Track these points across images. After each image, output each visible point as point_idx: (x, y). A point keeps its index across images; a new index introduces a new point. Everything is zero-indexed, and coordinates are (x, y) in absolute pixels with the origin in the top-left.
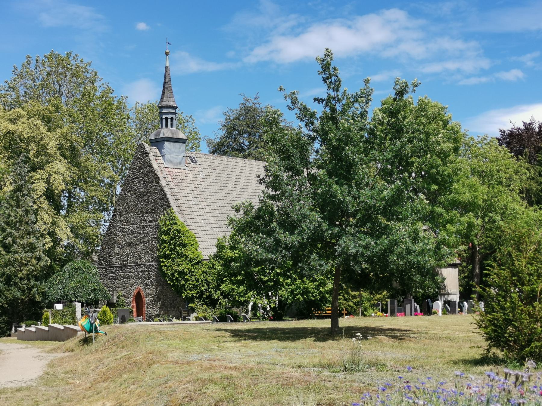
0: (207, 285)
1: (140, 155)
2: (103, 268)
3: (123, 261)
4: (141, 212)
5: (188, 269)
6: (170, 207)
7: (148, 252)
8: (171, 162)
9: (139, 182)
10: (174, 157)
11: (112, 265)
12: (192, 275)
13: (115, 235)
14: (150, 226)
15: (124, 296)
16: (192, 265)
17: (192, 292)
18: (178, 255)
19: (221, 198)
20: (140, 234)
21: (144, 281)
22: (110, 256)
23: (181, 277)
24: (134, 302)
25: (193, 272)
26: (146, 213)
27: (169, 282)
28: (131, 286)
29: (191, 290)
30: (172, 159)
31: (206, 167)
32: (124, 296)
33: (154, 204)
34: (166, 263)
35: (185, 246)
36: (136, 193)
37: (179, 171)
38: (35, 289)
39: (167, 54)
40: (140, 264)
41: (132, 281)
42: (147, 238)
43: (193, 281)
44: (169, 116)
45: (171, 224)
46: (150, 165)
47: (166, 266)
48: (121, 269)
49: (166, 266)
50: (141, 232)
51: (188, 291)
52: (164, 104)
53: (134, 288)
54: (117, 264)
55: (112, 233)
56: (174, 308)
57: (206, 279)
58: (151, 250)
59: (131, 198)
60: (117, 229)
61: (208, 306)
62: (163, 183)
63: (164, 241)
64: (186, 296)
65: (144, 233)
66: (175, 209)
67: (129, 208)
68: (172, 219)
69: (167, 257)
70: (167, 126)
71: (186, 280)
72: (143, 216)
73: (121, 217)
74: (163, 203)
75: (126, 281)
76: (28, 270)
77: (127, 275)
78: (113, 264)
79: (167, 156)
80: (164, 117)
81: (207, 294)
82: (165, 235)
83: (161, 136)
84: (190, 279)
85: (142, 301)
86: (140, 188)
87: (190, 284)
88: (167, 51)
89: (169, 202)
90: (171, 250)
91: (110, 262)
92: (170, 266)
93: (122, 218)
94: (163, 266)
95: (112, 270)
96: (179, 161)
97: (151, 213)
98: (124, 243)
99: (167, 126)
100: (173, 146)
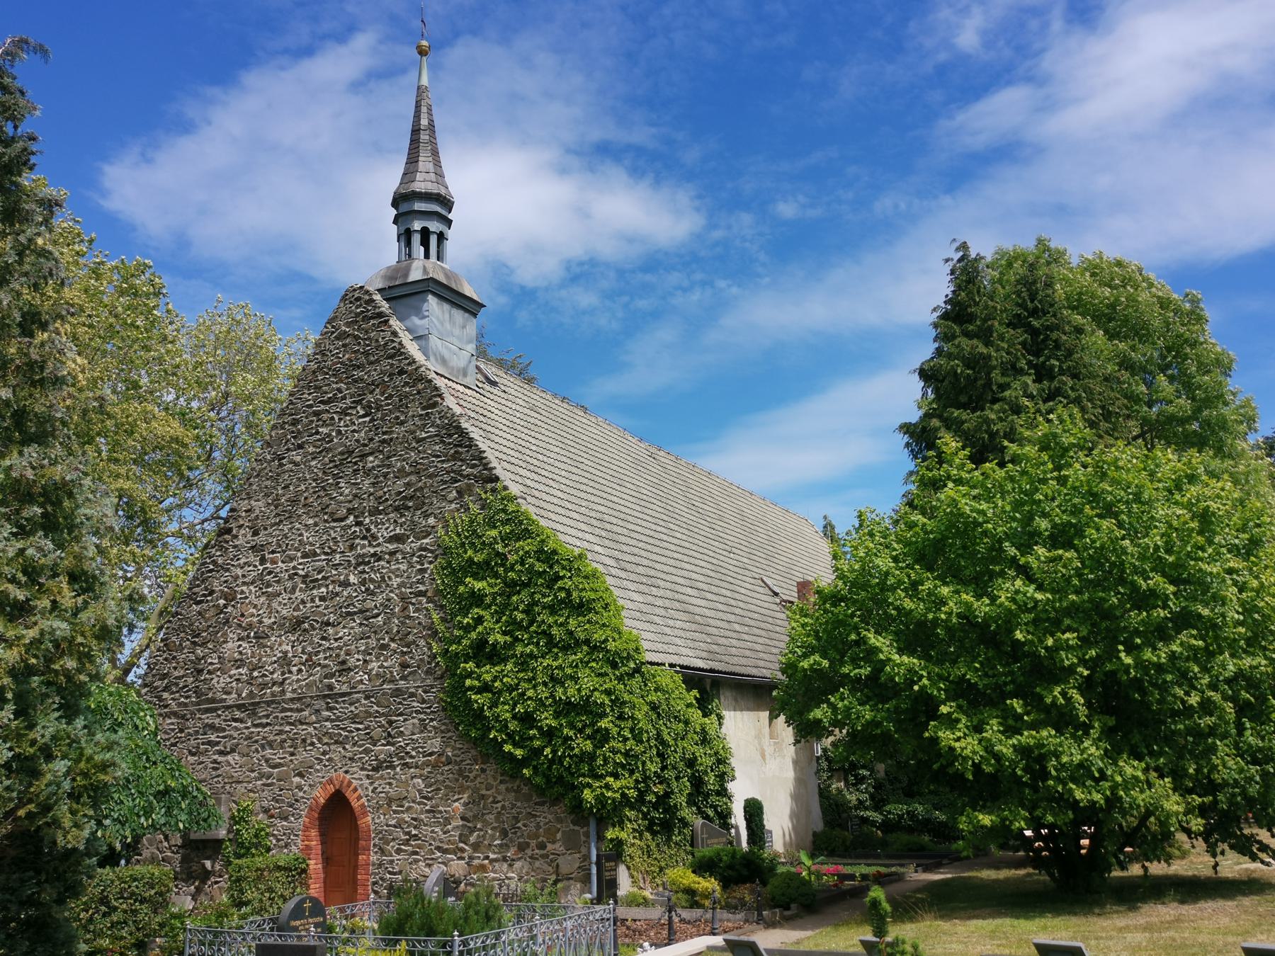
0: (660, 755)
1: (348, 324)
2: (167, 716)
3: (264, 686)
4: (350, 511)
5: (608, 692)
6: (497, 479)
7: (384, 647)
8: (444, 362)
9: (344, 413)
10: (450, 350)
11: (212, 705)
12: (621, 717)
13: (230, 597)
14: (392, 553)
15: (266, 811)
16: (620, 679)
17: (624, 782)
18: (551, 643)
19: (584, 487)
20: (346, 584)
21: (367, 751)
22: (200, 672)
23: (572, 726)
24: (314, 833)
25: (624, 703)
26: (374, 512)
27: (507, 748)
28: (301, 775)
29: (616, 776)
30: (446, 355)
31: (521, 402)
32: (266, 811)
33: (413, 478)
34: (488, 677)
35: (582, 608)
36: (328, 450)
37: (469, 392)
38: (61, 766)
39: (422, 52)
40: (345, 688)
41: (302, 755)
42: (380, 599)
43: (626, 739)
44: (434, 226)
45: (505, 539)
46: (400, 352)
47: (486, 688)
48: (254, 714)
49: (486, 688)
50: (352, 579)
51: (610, 780)
52: (420, 186)
53: (315, 778)
54: (231, 699)
55: (212, 593)
56: (522, 848)
57: (659, 735)
58: (403, 638)
59: (306, 466)
60: (236, 578)
61: (654, 834)
62: (450, 402)
63: (476, 599)
64: (601, 800)
65: (363, 583)
66: (515, 489)
67: (294, 502)
68: (507, 522)
69: (484, 652)
70: (427, 256)
71: (601, 738)
72: (358, 524)
73: (255, 533)
74: (459, 473)
75: (276, 756)
76: (36, 642)
77: (281, 732)
78: (213, 700)
79: (434, 341)
80: (417, 225)
81: (659, 789)
82: (476, 577)
83: (415, 275)
84: (615, 730)
85: (357, 826)
86: (355, 428)
87: (614, 751)
88: (424, 43)
89: (486, 466)
90: (513, 627)
91: (197, 692)
92: (511, 689)
93: (261, 539)
94: (471, 688)
95: (208, 719)
96: (462, 364)
97: (397, 509)
98: (267, 621)
99: (427, 256)
100: (447, 316)
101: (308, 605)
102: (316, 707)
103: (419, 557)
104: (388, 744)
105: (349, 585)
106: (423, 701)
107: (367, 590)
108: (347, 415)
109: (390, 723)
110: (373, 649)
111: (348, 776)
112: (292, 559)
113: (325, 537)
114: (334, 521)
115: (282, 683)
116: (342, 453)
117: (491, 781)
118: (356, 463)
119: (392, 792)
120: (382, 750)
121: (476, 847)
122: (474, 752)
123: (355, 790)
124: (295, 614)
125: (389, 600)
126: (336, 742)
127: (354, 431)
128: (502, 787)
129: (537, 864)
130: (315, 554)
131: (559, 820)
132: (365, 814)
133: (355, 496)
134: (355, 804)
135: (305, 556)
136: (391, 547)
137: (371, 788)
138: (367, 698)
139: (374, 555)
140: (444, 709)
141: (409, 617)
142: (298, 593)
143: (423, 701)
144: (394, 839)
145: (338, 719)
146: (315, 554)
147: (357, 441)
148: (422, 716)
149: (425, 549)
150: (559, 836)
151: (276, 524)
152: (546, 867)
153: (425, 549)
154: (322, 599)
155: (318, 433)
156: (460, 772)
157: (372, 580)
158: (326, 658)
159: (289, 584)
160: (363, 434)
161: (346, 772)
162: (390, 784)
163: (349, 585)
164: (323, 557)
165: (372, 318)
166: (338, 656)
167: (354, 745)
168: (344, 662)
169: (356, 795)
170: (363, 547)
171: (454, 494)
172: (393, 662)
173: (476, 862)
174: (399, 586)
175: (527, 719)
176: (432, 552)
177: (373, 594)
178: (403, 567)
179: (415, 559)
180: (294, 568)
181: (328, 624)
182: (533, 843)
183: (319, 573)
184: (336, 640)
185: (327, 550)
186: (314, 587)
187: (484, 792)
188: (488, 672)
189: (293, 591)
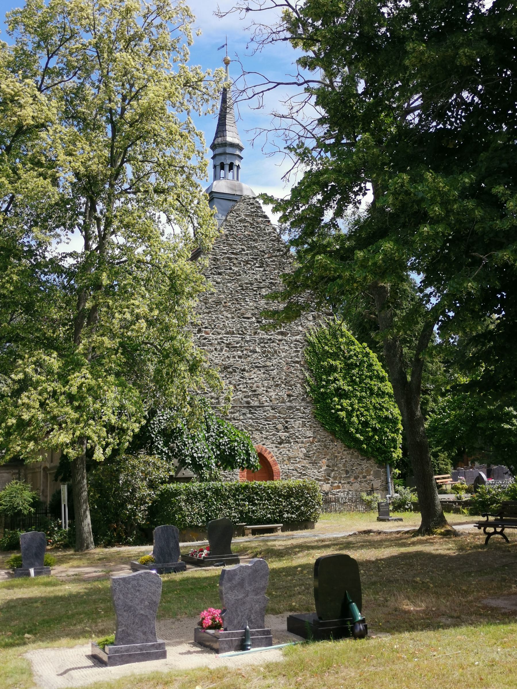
7: (277, 385)
20: (254, 352)
21: (274, 435)
40: (257, 404)
50: (258, 350)
56: (356, 478)
65: (264, 352)
67: (218, 303)
72: (258, 322)
101: (231, 359)
102: (244, 412)
103: (295, 344)
104: (285, 432)
105: (256, 352)
106: (304, 413)
107: (267, 356)
108: (248, 263)
109: (287, 422)
110: (272, 386)
111: (265, 446)
112: (219, 334)
113: (239, 326)
114: (244, 318)
115: (217, 399)
116: (247, 283)
117: (339, 450)
118: (254, 291)
119: (290, 455)
120: (283, 435)
121: (335, 478)
122: (331, 437)
123: (270, 453)
124: (224, 363)
125: (280, 363)
126: (257, 430)
127: (254, 273)
128: (345, 453)
129: (363, 484)
130: (233, 333)
131: (372, 466)
132: (276, 464)
133: (256, 308)
134: (270, 460)
135: (227, 333)
136: (280, 337)
137: (278, 452)
138: (273, 409)
139: (270, 339)
140: (315, 417)
141: (291, 372)
142: (224, 352)
143: (304, 413)
144: (293, 476)
145: (257, 418)
146: (233, 333)
147: (256, 279)
148: (304, 420)
149: (298, 341)
150: (372, 473)
151: (206, 313)
152: (366, 485)
153: (298, 341)
154: (240, 357)
155: (231, 269)
156: (325, 446)
157: (269, 352)
158: (244, 388)
159: (218, 347)
160: (258, 277)
161: (264, 444)
162: (289, 450)
163: (256, 352)
164: (239, 336)
165: (260, 217)
166: (251, 387)
167: (267, 431)
168: (255, 391)
169: (270, 455)
170: (262, 334)
171: (311, 318)
172: (283, 394)
173: (336, 485)
174: (285, 357)
175: (366, 424)
176: (302, 343)
177: (270, 359)
178: (287, 348)
179: (292, 345)
180: (221, 338)
181: (244, 370)
182: (361, 476)
183: (237, 343)
184: (250, 379)
185: (240, 332)
186: (234, 351)
187: (336, 454)
188: (345, 403)
189: (221, 350)
